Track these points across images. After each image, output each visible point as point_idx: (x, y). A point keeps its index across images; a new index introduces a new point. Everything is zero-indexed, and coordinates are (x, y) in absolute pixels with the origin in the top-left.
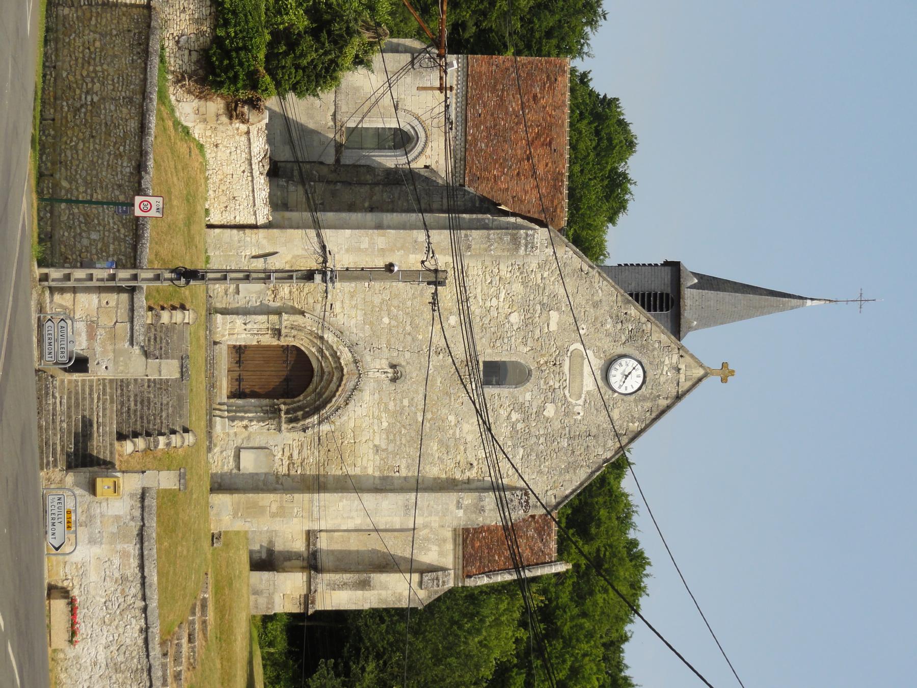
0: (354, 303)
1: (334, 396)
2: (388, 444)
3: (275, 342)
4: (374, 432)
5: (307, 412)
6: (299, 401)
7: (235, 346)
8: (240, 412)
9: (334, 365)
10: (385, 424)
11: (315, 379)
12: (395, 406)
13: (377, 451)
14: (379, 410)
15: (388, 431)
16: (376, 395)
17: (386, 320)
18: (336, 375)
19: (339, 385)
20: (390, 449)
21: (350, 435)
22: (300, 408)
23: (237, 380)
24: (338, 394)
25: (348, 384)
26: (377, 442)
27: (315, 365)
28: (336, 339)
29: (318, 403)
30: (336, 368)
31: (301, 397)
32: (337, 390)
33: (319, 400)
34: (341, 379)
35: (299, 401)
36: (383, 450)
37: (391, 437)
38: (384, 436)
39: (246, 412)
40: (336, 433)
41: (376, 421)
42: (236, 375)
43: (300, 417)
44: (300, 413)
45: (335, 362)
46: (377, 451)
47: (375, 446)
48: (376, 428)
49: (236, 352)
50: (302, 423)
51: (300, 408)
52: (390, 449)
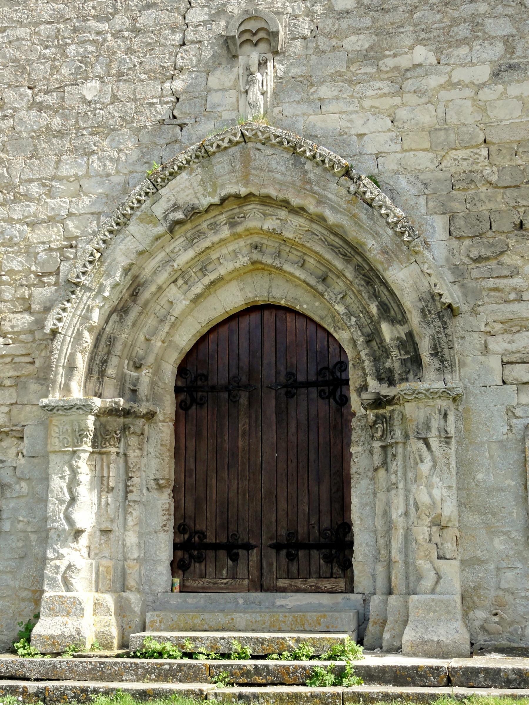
0: (34, 189)
1: (321, 219)
2: (490, 39)
3: (164, 431)
4: (451, 85)
5: (384, 308)
6: (354, 342)
7: (178, 566)
8: (388, 545)
9: (225, 232)
10: (422, 54)
11: (281, 293)
12: (358, 31)
13: (512, 67)
14: (372, 78)
15: (444, 43)
16: (325, 91)
17: (90, 89)
18: (255, 219)
19: (285, 204)
20: (500, 28)
21: (458, 160)
22: (373, 337)
23: (291, 558)
24: (312, 208)
25: (274, 174)
26: (483, 73)
27: (231, 299)
28: (133, 227)
29: (349, 273)
30: (232, 224)
31: (343, 336)
32: (299, 211)
33: (340, 275)
34: (266, 200)
35: (354, 342)
36: (510, 49)
37: (463, 31)
38: (463, 51)
39: (389, 526)
40: (457, 206)
41: (409, 85)
42: (275, 561)
43: (401, 331)
44: (388, 332)
45: (214, 227)
46: (512, 67)
47: (496, 75)
48: (434, 81)
49: (200, 559)
50: (415, 319)
51: (373, 337)
52: (500, 28)
